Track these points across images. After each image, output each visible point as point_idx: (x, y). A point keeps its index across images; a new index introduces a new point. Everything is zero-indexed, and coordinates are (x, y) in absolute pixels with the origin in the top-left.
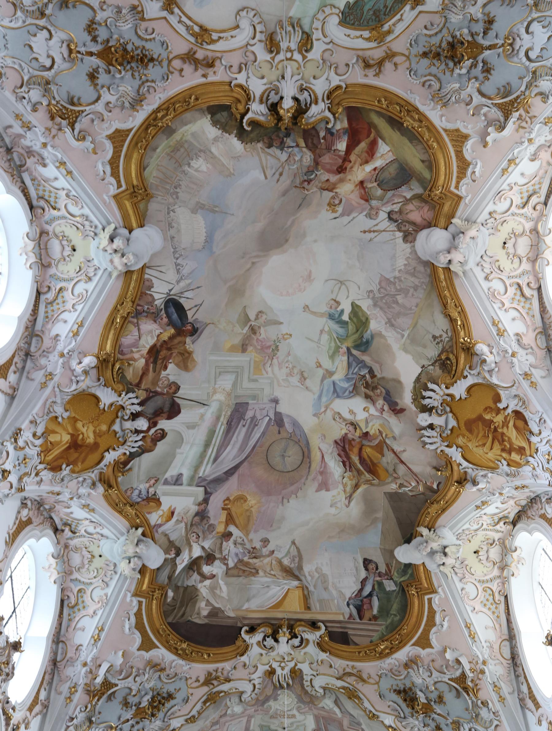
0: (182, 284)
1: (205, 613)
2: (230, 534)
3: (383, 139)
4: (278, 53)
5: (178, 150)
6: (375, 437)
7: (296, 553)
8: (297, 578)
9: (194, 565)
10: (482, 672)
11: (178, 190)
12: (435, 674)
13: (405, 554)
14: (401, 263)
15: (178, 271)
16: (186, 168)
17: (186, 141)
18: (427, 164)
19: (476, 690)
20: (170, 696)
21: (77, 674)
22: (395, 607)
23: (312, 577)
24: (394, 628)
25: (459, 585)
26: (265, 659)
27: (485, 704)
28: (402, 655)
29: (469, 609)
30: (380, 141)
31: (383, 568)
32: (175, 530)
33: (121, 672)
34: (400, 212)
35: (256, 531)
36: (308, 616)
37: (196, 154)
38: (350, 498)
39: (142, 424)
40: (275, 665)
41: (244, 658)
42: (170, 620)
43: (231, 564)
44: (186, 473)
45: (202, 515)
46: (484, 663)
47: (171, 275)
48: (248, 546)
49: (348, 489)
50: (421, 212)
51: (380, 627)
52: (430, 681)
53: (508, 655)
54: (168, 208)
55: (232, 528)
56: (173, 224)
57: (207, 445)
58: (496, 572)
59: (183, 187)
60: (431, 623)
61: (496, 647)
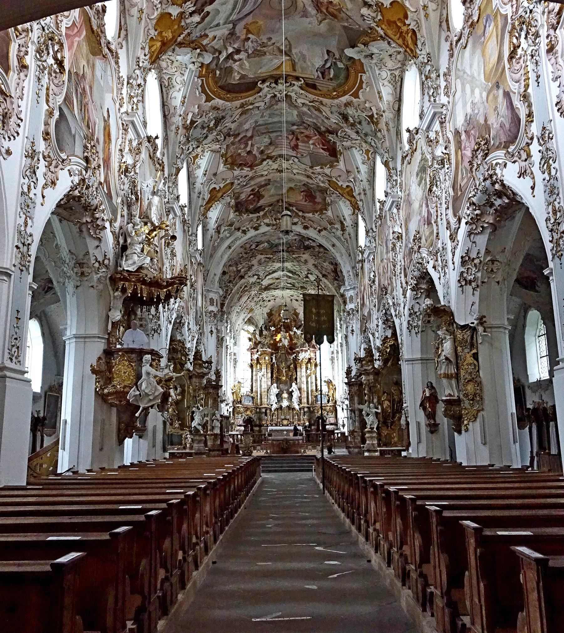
1: (238, 78)
2: (249, 38)
6: (335, 5)
7: (288, 43)
8: (289, 56)
9: (230, 57)
10: (382, 116)
12: (359, 111)
13: (349, 52)
19: (377, 124)
20: (223, 117)
21: (177, 120)
22: (343, 75)
23: (297, 56)
24: (340, 86)
25: (377, 72)
26: (271, 92)
27: (380, 131)
28: (344, 99)
29: (381, 84)
31: (337, 56)
32: (217, 44)
33: (198, 114)
35: (264, 35)
36: (294, 74)
38: (320, 22)
39: (197, 18)
40: (276, 93)
41: (261, 94)
42: (219, 84)
43: (250, 52)
44: (221, 22)
45: (232, 34)
46: (384, 112)
48: (260, 42)
49: (320, 19)
51: (334, 84)
52: (356, 114)
53: (396, 109)
55: (250, 36)
57: (234, 9)
58: (399, 65)
60: (360, 87)
61: (391, 104)
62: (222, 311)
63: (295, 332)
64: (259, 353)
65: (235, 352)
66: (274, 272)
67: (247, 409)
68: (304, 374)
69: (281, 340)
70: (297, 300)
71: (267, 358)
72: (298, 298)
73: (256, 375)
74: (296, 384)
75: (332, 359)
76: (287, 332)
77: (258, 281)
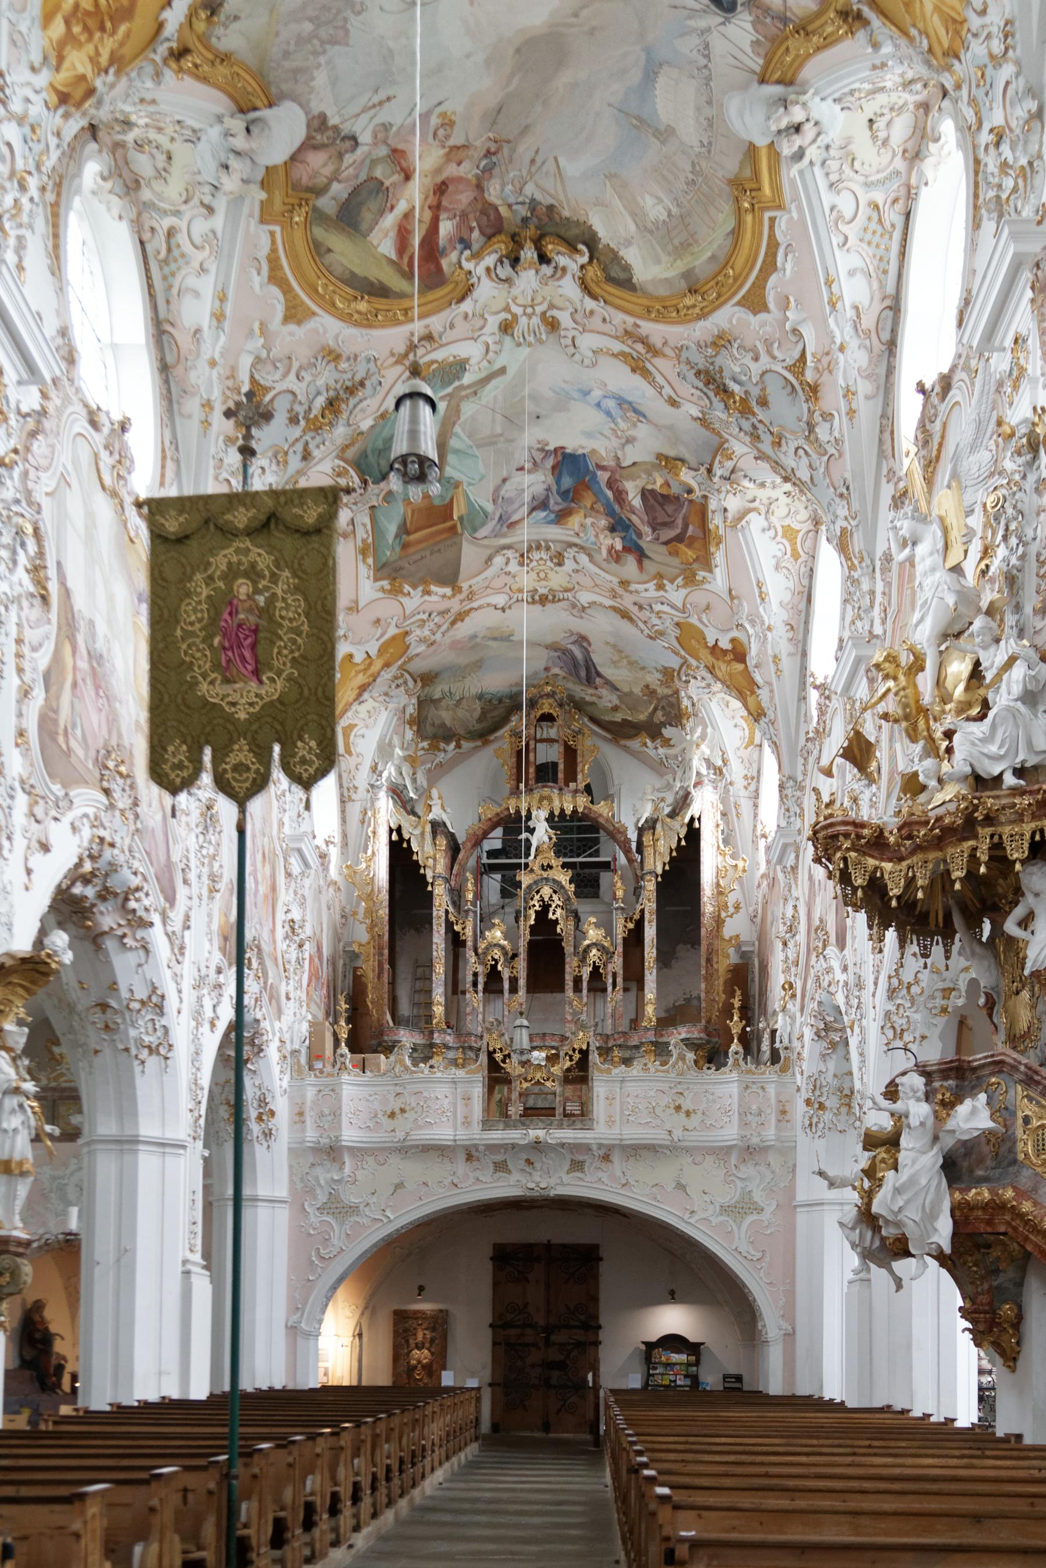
0: (702, 23)
3: (390, 261)
4: (544, 314)
5: (681, 244)
11: (691, 176)
14: (321, 79)
15: (707, 46)
16: (675, 210)
17: (669, 254)
18: (323, 249)
30: (394, 257)
34: (340, 156)
37: (658, 228)
47: (718, 46)
50: (309, 170)
54: (709, 152)
56: (705, 123)
59: (683, 180)
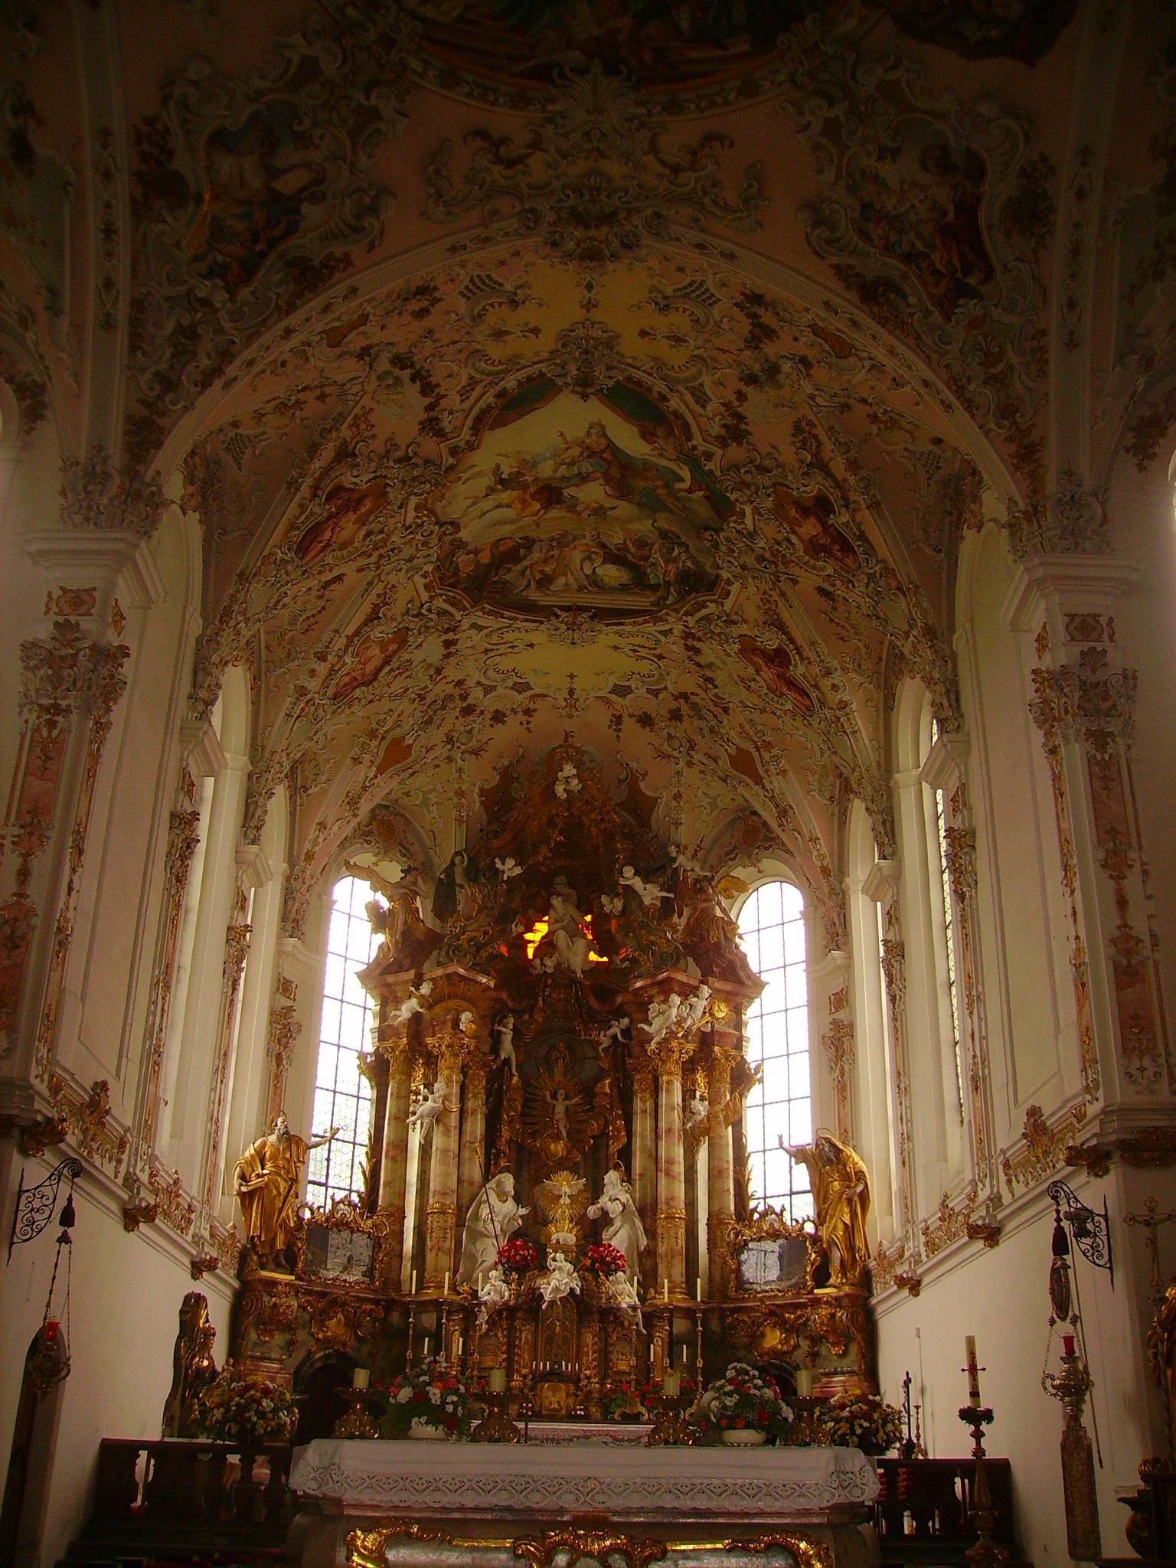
62: (132, 472)
63: (630, 890)
64: (426, 989)
65: (289, 972)
66: (532, 394)
67: (327, 1301)
68: (677, 1116)
69: (547, 945)
70: (646, 721)
71: (466, 1017)
72: (650, 705)
73: (402, 1118)
74: (627, 1177)
75: (835, 1042)
76: (584, 907)
77: (430, 446)
